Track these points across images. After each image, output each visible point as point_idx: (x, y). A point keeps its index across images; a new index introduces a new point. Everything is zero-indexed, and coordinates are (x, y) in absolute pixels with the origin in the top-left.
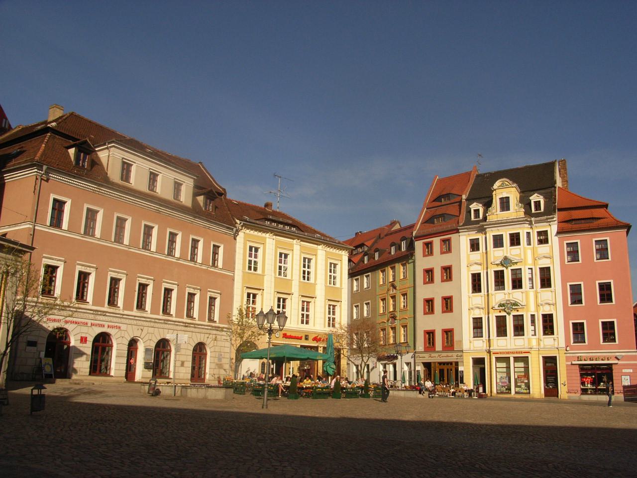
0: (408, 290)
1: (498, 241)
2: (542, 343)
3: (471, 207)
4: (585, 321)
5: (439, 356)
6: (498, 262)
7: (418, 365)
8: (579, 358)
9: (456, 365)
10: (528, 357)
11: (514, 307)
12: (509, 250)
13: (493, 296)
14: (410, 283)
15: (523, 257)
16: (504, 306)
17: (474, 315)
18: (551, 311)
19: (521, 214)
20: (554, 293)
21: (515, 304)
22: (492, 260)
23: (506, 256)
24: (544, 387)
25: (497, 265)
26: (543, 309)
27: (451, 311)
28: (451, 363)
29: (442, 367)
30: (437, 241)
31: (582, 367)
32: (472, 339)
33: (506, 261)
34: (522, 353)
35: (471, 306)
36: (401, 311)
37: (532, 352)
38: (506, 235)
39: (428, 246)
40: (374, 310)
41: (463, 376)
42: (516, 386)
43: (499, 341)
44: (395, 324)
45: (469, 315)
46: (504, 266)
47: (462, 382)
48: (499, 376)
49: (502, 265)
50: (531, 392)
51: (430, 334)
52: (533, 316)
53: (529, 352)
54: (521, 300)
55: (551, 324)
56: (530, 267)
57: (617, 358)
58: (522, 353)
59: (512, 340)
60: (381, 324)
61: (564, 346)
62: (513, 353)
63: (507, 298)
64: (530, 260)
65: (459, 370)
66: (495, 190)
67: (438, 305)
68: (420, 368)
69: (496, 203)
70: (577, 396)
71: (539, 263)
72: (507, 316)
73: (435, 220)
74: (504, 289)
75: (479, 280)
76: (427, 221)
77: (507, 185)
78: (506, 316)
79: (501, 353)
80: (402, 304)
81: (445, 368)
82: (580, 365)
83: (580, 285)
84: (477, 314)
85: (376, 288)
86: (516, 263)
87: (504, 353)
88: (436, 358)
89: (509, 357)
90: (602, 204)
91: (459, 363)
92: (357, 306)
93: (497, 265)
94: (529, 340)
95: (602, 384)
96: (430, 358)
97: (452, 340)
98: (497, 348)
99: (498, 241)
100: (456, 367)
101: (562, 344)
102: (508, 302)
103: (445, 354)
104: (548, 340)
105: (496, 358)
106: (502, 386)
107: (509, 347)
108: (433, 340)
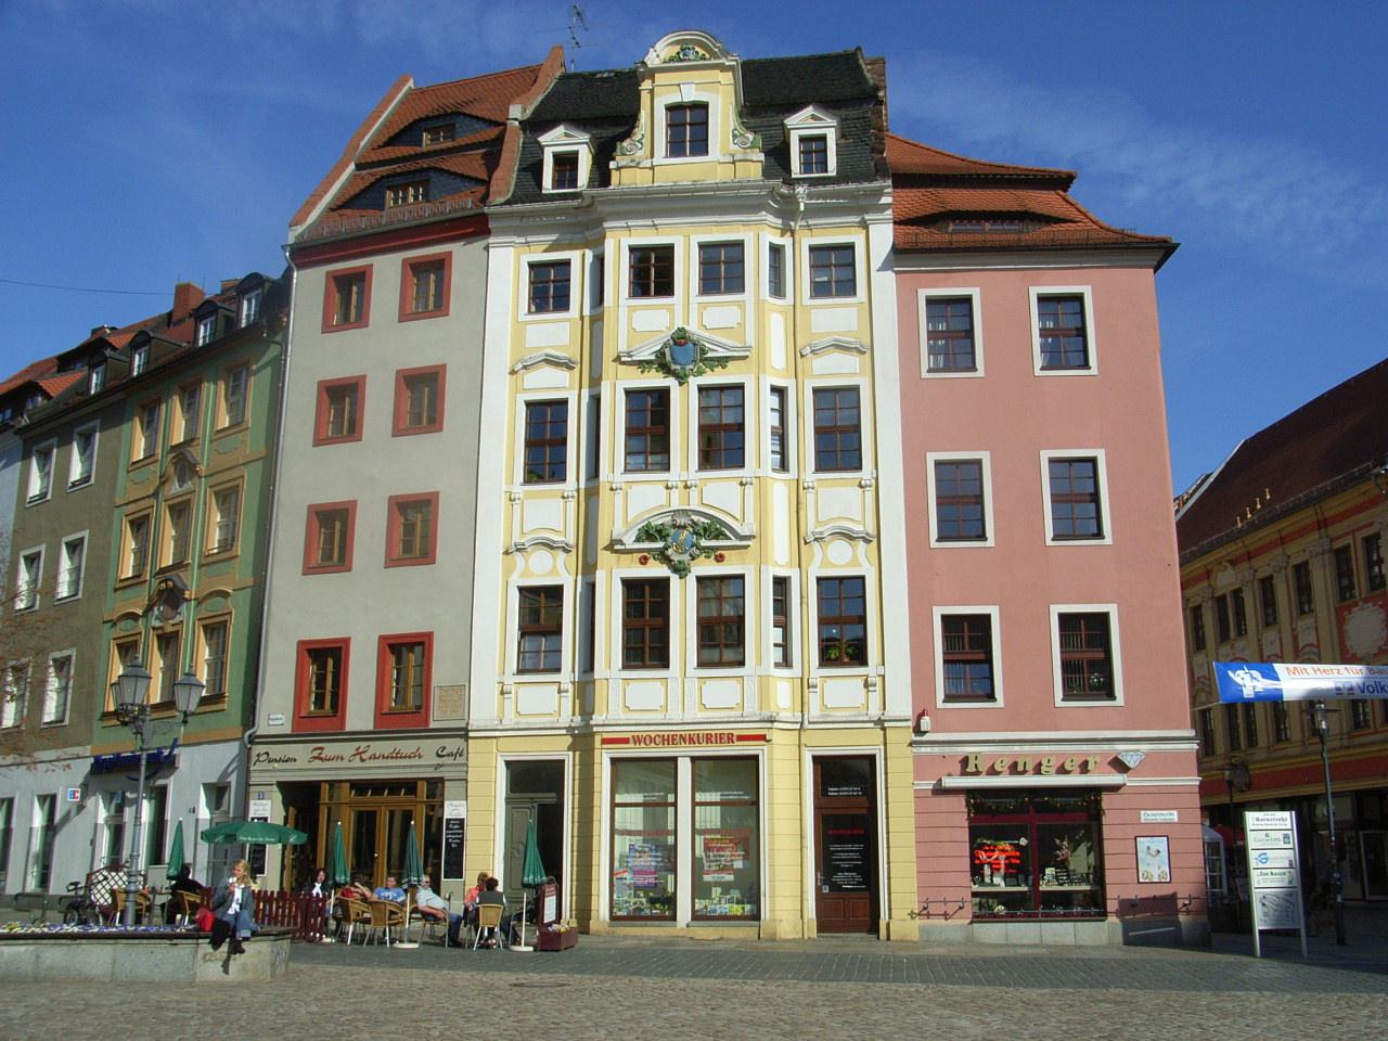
0: (246, 472)
1: (653, 272)
2: (813, 700)
4: (994, 611)
5: (358, 753)
6: (647, 354)
7: (261, 796)
9: (431, 794)
10: (756, 758)
11: (704, 543)
13: (619, 496)
15: (750, 340)
16: (663, 538)
17: (524, 574)
19: (753, 168)
20: (870, 494)
21: (715, 529)
22: (623, 347)
24: (818, 890)
25: (643, 365)
26: (824, 557)
27: (427, 556)
28: (410, 786)
30: (387, 271)
31: (979, 800)
32: (511, 679)
33: (680, 353)
34: (730, 738)
35: (517, 538)
36: (208, 562)
37: (775, 736)
40: (95, 573)
41: (461, 845)
42: (700, 890)
44: (178, 619)
45: (508, 571)
48: (622, 844)
49: (665, 368)
50: (765, 913)
51: (326, 658)
52: (781, 584)
53: (762, 738)
56: (780, 383)
57: (1119, 765)
58: (730, 738)
59: (692, 686)
60: (123, 624)
62: (691, 740)
63: (675, 506)
65: (446, 816)
67: (370, 533)
68: (267, 807)
69: (653, 121)
70: (956, 929)
71: (816, 371)
72: (675, 580)
73: (389, 195)
74: (666, 467)
76: (357, 196)
78: (667, 580)
79: (637, 740)
80: (215, 537)
81: (383, 806)
82: (970, 792)
83: (979, 463)
84: (545, 569)
85: (115, 477)
86: (722, 361)
87: (653, 740)
89: (674, 760)
92: (32, 560)
93: (643, 365)
94: (764, 683)
95: (1050, 871)
96: (317, 764)
97: (424, 685)
98: (623, 717)
99: (653, 272)
101: (901, 705)
102: (681, 521)
104: (842, 689)
106: (637, 888)
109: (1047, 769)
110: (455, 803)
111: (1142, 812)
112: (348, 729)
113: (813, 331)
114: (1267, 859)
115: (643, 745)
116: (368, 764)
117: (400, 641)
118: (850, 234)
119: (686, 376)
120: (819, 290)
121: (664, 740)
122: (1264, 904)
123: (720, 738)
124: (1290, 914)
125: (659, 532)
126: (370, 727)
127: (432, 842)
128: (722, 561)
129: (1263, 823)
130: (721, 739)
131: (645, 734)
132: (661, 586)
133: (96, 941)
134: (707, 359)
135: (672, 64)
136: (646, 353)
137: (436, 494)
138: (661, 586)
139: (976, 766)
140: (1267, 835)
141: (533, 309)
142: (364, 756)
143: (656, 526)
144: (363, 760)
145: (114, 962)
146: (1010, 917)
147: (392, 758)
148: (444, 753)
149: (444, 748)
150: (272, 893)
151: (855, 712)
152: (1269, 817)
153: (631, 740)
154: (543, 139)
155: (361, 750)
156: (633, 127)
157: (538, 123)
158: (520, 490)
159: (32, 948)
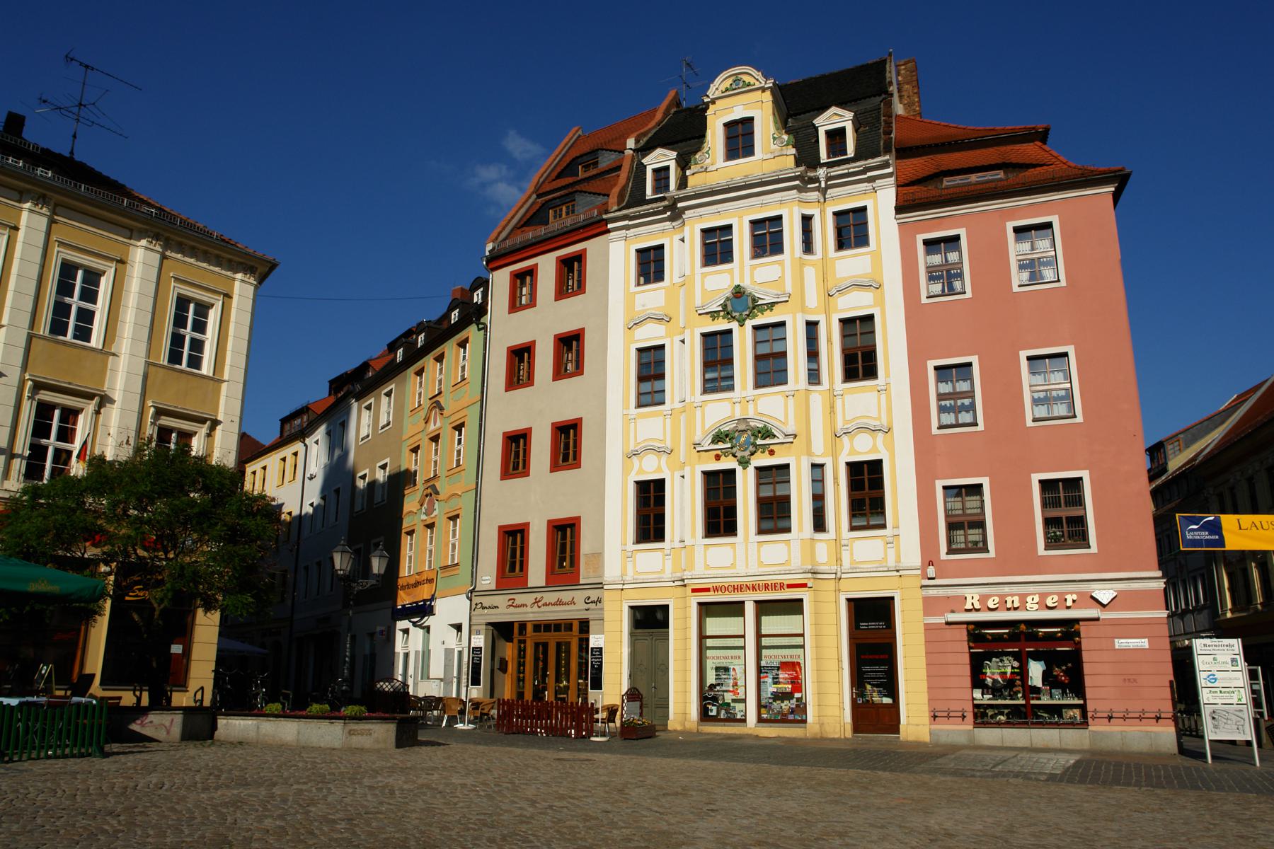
3: (645, 161)
5: (537, 602)
7: (478, 633)
11: (759, 442)
12: (747, 270)
14: (473, 391)
17: (638, 473)
19: (787, 161)
25: (714, 315)
28: (568, 626)
29: (543, 636)
34: (782, 586)
35: (632, 447)
39: (525, 278)
43: (711, 549)
45: (626, 471)
46: (734, 318)
47: (597, 684)
49: (729, 315)
51: (514, 537)
53: (804, 585)
55: (874, 493)
58: (782, 586)
59: (753, 548)
61: (917, 562)
63: (738, 416)
64: (813, 298)
65: (591, 645)
66: (713, 102)
70: (960, 731)
77: (749, 85)
78: (733, 472)
79: (716, 589)
81: (552, 638)
87: (727, 589)
88: (528, 610)
89: (743, 602)
93: (714, 315)
100: (584, 636)
101: (912, 555)
102: (742, 427)
103: (550, 597)
105: (700, 604)
107: (741, 570)
108: (522, 555)
109: (1032, 606)
110: (596, 636)
111: (1116, 640)
112: (529, 586)
113: (838, 276)
114: (1216, 679)
115: (720, 592)
118: (863, 199)
119: (744, 320)
120: (841, 244)
122: (1214, 718)
124: (1240, 727)
127: (583, 666)
129: (1211, 648)
131: (721, 585)
132: (731, 473)
133: (265, 718)
135: (728, 93)
136: (715, 306)
138: (731, 473)
140: (1214, 659)
141: (642, 279)
142: (540, 604)
143: (725, 432)
145: (299, 733)
146: (1008, 724)
149: (589, 598)
150: (513, 700)
151: (877, 565)
152: (1217, 644)
153: (712, 590)
154: (645, 161)
156: (702, 143)
157: (645, 150)
158: (633, 411)
159: (255, 722)
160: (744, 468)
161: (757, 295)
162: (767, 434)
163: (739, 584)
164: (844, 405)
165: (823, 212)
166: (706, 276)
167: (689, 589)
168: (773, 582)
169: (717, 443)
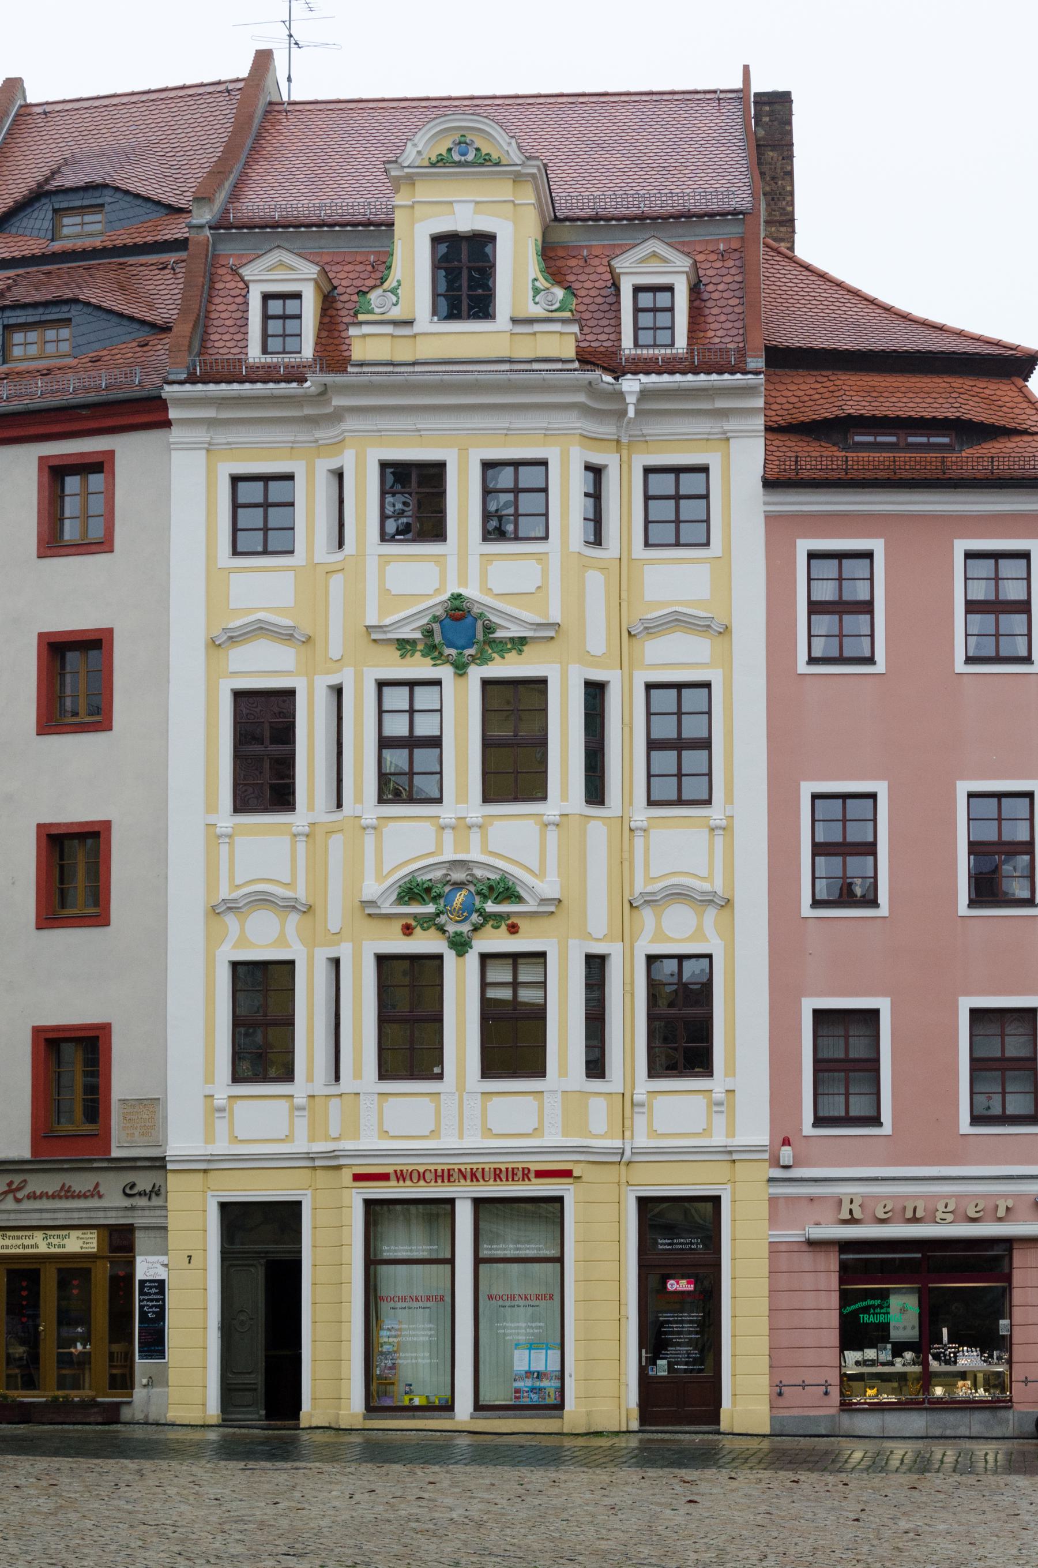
8: (846, 1206)
10: (560, 1200)
11: (490, 907)
12: (474, 563)
16: (435, 899)
18: (706, 939)
23: (458, 597)
25: (405, 646)
34: (526, 1174)
35: (224, 893)
38: (463, 470)
41: (161, 1316)
45: (212, 941)
49: (432, 650)
53: (567, 1174)
54: (535, 867)
58: (526, 1174)
59: (473, 1106)
61: (764, 1140)
62: (473, 1176)
63: (449, 855)
65: (140, 1274)
75: (286, 733)
78: (440, 957)
79: (401, 1176)
86: (520, 643)
87: (422, 1176)
89: (451, 1202)
90: (1001, 351)
91: (139, 1235)
93: (405, 646)
102: (459, 876)
107: (449, 1141)
110: (150, 1258)
115: (408, 1183)
116: (27, 1205)
117: (61, 1035)
121: (436, 1176)
123: (511, 1175)
125: (428, 890)
126: (26, 1154)
128: (516, 932)
130: (513, 1174)
131: (410, 1168)
134: (494, 641)
136: (407, 629)
137: (107, 824)
139: (851, 1211)
142: (19, 1195)
144: (18, 1201)
147: (60, 1197)
148: (135, 1191)
149: (133, 1186)
153: (393, 1177)
155: (14, 1186)
160: (461, 954)
161: (494, 619)
162: (505, 895)
163: (446, 1167)
164: (647, 850)
165: (624, 467)
166: (388, 562)
167: (347, 1175)
168: (510, 1166)
169: (406, 903)
